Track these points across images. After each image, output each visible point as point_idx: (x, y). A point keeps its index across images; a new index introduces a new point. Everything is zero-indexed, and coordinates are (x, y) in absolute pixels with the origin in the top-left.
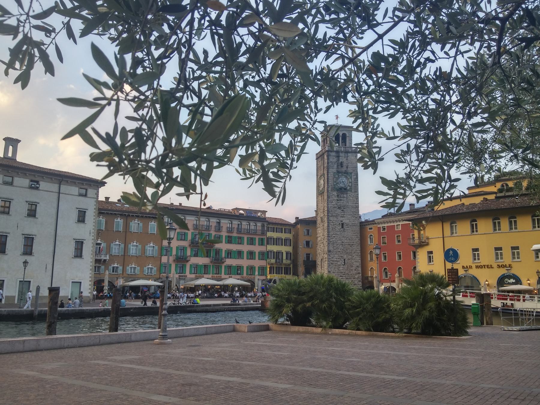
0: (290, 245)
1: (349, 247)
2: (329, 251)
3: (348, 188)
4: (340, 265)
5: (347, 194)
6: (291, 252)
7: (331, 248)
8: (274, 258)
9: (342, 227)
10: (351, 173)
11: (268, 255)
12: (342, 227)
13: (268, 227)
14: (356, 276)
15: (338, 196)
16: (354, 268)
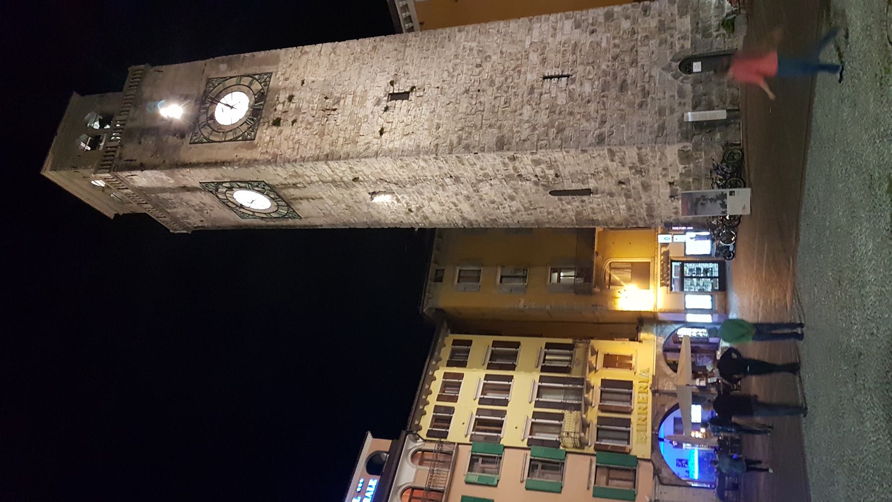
0: (517, 345)
1: (487, 66)
2: (501, 145)
3: (257, 86)
4: (571, 97)
5: (277, 91)
6: (543, 341)
7: (490, 137)
8: (561, 417)
9: (404, 96)
10: (209, 81)
11: (543, 443)
12: (404, 96)
13: (430, 434)
14: (626, 25)
15: (277, 123)
16: (586, 40)
